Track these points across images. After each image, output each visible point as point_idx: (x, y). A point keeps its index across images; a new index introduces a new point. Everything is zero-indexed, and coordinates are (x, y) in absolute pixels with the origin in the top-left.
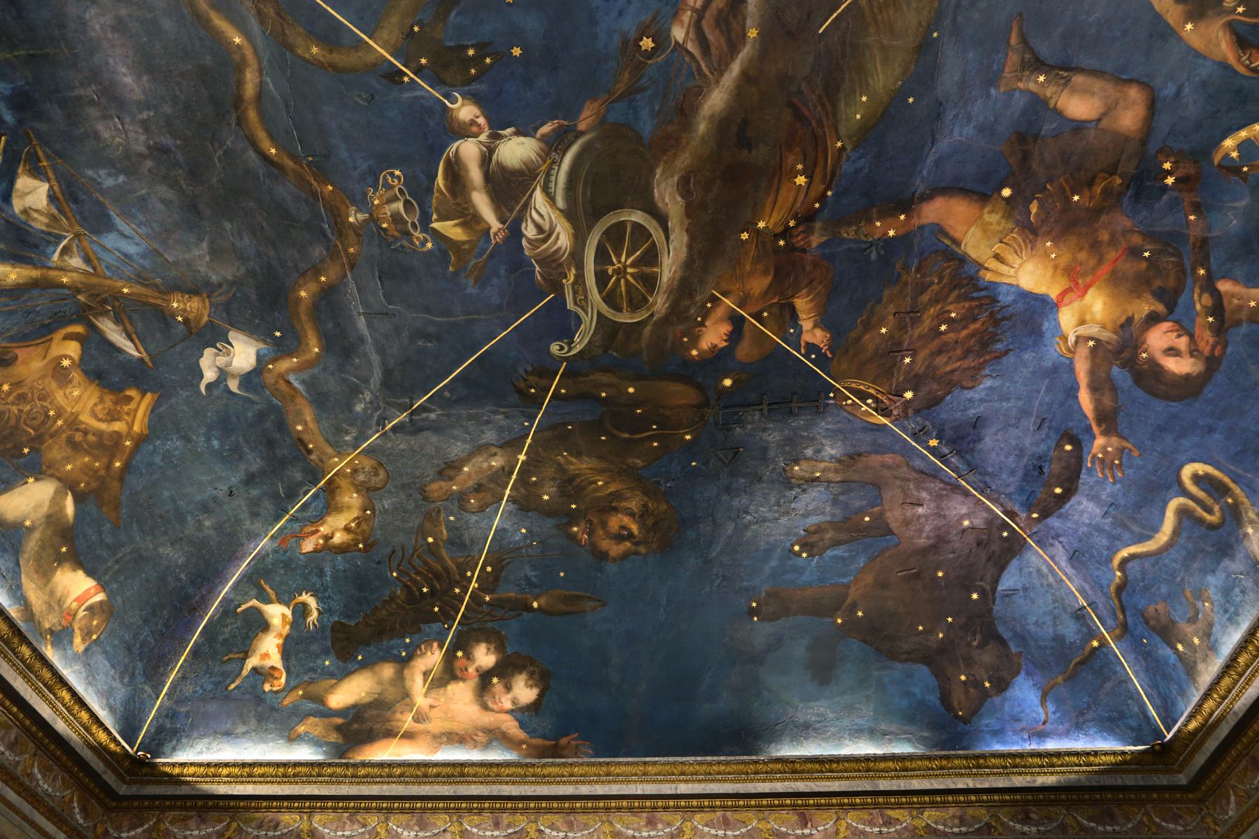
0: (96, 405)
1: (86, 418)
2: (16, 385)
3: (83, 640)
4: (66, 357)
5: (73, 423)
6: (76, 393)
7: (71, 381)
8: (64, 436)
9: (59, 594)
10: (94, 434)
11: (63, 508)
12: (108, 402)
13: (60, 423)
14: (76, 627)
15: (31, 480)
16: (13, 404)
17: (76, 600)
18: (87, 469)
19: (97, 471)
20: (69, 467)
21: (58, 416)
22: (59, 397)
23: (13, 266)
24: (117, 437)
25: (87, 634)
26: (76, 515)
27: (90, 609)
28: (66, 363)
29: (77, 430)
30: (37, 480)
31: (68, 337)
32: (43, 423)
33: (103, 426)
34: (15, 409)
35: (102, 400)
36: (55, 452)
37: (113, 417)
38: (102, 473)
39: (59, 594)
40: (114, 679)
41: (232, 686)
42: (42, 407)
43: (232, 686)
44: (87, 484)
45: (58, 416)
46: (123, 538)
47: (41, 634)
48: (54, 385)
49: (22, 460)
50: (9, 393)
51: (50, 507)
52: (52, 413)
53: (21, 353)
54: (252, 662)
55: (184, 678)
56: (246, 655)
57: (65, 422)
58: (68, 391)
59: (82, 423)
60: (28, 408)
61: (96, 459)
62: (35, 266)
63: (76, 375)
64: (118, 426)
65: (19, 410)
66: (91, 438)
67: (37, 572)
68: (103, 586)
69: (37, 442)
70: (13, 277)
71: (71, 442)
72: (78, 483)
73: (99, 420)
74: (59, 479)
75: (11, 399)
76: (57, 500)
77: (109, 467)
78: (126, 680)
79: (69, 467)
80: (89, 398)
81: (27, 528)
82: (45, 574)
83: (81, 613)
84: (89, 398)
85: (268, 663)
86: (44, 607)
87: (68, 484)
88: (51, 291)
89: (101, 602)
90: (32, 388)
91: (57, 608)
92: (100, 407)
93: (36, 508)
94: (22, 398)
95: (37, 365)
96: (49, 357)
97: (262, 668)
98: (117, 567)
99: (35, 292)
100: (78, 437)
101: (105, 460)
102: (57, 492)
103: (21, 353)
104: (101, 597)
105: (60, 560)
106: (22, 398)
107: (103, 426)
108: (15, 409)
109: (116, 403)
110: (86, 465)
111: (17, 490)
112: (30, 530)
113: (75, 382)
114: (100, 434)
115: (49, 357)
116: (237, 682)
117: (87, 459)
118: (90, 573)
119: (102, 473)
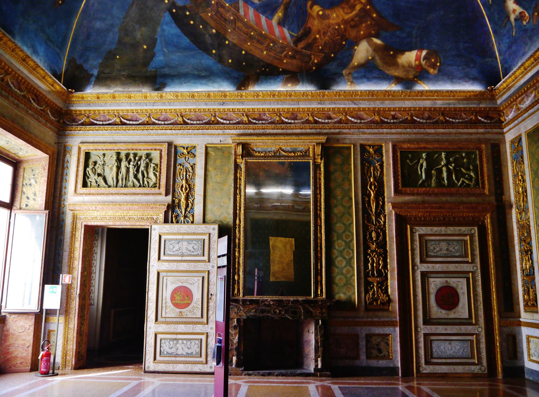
0: (344, 11)
1: (347, 17)
2: (319, 32)
3: (434, 69)
4: (318, 12)
5: (345, 22)
6: (335, 15)
7: (329, 15)
8: (348, 28)
9: (406, 65)
10: (356, 17)
11: (376, 44)
12: (346, 6)
13: (342, 26)
14: (426, 67)
15: (356, 47)
16: (324, 37)
17: (416, 60)
18: (367, 27)
19: (371, 24)
20: (362, 33)
21: (339, 25)
22: (332, 21)
23: (277, 12)
24: (363, 10)
25: (434, 66)
26: (383, 41)
27: (425, 58)
28: (321, 13)
29: (349, 22)
30: (357, 46)
31: (311, 7)
32: (338, 32)
33: (354, 13)
34: (327, 38)
35: (343, 8)
36: (353, 33)
37: (353, 7)
38: (373, 23)
39: (406, 65)
40: (464, 69)
41: (514, 33)
42: (333, 29)
43: (514, 33)
44: (374, 30)
45: (339, 25)
46: (408, 30)
47: (411, 81)
48: (327, 21)
49: (346, 46)
50: (320, 36)
51: (371, 48)
52: (337, 27)
53: (309, 25)
54: (512, 17)
55: (499, 44)
56: (508, 17)
57: (343, 24)
58: (332, 17)
59: (347, 19)
60: (329, 34)
61: (366, 22)
62: (280, 6)
63: (327, 12)
64: (358, 7)
65: (328, 37)
66: (357, 19)
67: (390, 66)
68: (421, 49)
69: (343, 37)
70: (280, 14)
71: (352, 27)
72: (371, 33)
73: (351, 12)
74: (364, 38)
75: (322, 37)
76: (371, 44)
77: (373, 19)
78: (472, 65)
79: (362, 33)
80: (339, 12)
81: (372, 59)
82: (395, 64)
83: (423, 63)
84: (339, 12)
85: (517, 13)
86: (405, 73)
87: (368, 37)
88: (291, 5)
89: (427, 53)
90: (323, 28)
91: (410, 69)
92: (345, 10)
93: (367, 51)
94: (325, 34)
95: (316, 22)
96: (315, 17)
97: (517, 16)
98: (418, 39)
99: (289, 10)
100: (352, 23)
101: (369, 19)
102: (368, 42)
103: (309, 25)
104: (424, 53)
105: (395, 57)
106: (325, 34)
107: (354, 13)
108: (327, 38)
109: (347, 4)
110: (366, 26)
111: (356, 53)
112: (373, 58)
113: (330, 13)
114: (357, 15)
115: (315, 17)
116: (514, 30)
117: (364, 25)
118: (410, 50)
119: (373, 23)
